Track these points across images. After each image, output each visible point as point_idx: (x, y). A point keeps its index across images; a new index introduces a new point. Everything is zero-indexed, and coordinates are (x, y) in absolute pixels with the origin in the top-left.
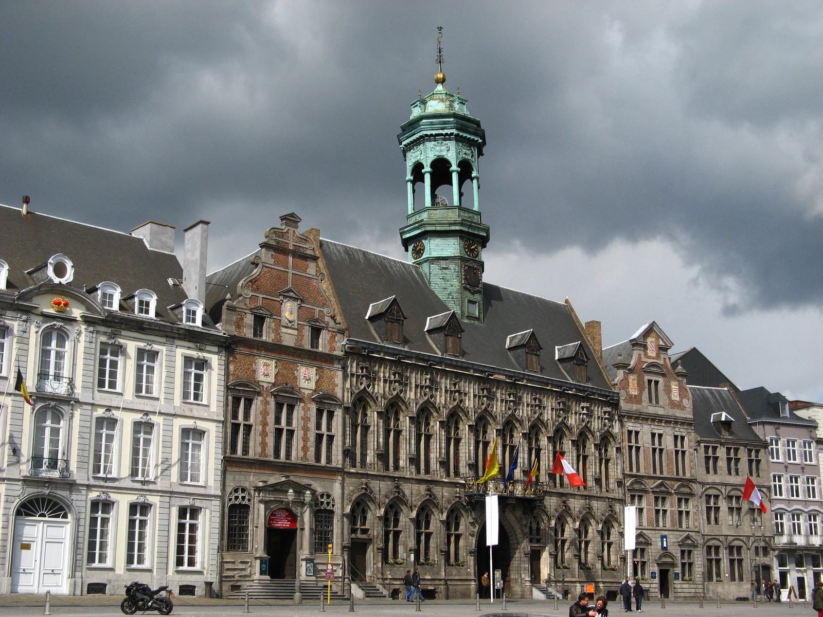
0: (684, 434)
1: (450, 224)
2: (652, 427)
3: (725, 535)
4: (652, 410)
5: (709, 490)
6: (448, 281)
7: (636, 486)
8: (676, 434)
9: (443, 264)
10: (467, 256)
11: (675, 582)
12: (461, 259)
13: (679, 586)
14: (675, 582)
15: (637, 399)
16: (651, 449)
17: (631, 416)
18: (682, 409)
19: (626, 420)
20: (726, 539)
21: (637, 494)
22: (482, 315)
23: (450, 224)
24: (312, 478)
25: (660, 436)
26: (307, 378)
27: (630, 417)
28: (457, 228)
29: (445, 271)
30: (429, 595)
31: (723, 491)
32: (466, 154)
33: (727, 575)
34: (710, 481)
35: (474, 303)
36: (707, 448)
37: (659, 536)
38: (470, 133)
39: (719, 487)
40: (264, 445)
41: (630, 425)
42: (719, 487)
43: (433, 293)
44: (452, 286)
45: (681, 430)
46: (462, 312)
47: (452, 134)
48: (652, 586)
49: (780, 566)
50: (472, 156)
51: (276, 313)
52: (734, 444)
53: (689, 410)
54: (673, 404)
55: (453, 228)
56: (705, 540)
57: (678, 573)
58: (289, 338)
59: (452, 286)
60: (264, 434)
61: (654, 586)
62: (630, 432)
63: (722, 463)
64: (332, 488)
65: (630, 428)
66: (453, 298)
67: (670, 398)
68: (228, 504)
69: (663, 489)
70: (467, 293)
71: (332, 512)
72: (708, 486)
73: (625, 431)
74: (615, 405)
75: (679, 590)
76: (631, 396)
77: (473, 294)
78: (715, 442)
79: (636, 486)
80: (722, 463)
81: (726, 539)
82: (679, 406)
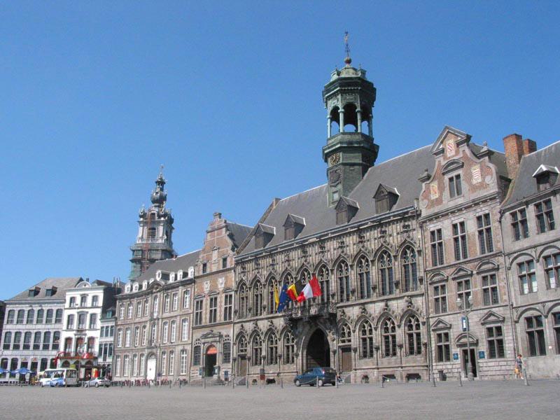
0: (487, 212)
2: (453, 219)
3: (541, 303)
4: (452, 204)
5: (520, 258)
7: (436, 279)
8: (477, 215)
11: (479, 361)
13: (485, 365)
14: (479, 361)
15: (439, 201)
16: (452, 240)
17: (431, 219)
18: (484, 188)
19: (428, 223)
20: (544, 307)
21: (439, 285)
24: (221, 329)
25: (462, 224)
26: (221, 282)
27: (431, 219)
30: (271, 381)
31: (533, 254)
33: (550, 347)
34: (517, 248)
35: (336, 192)
36: (514, 215)
37: (460, 318)
39: (528, 252)
40: (206, 318)
41: (432, 227)
42: (528, 252)
45: (484, 209)
48: (454, 366)
49: (542, 330)
51: (209, 259)
52: (541, 198)
53: (493, 185)
54: (474, 188)
56: (519, 313)
57: (483, 352)
58: (214, 269)
60: (206, 313)
61: (458, 366)
62: (433, 233)
63: (532, 223)
64: (230, 331)
65: (432, 230)
67: (471, 184)
68: (194, 346)
69: (462, 273)
70: (333, 188)
71: (229, 343)
72: (515, 255)
73: (428, 234)
74: (417, 215)
75: (485, 369)
76: (433, 201)
77: (335, 186)
78: (521, 204)
79: (436, 279)
80: (532, 223)
81: (544, 307)
82: (482, 185)
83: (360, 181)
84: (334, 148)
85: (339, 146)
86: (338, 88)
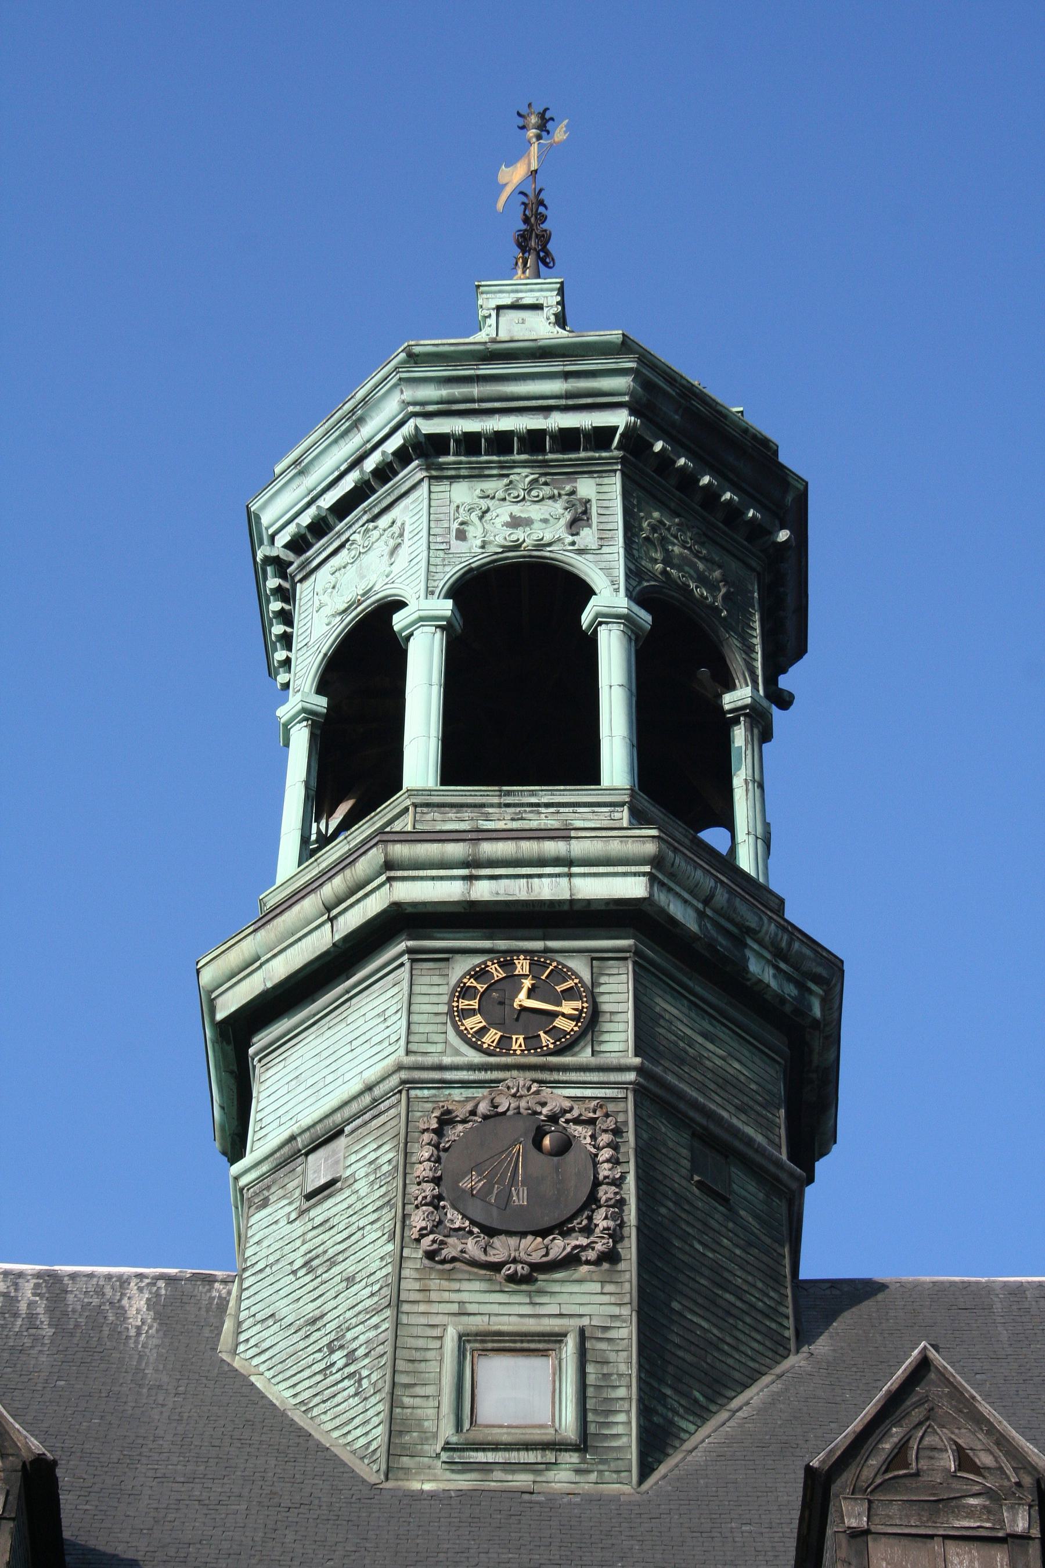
1: (330, 911)
6: (332, 1262)
9: (317, 1169)
10: (475, 1057)
12: (411, 1078)
22: (624, 1428)
23: (330, 911)
28: (372, 906)
29: (319, 1214)
32: (516, 522)
35: (536, 1344)
38: (547, 410)
43: (241, 1383)
44: (350, 1281)
46: (396, 1427)
47: (403, 456)
50: (579, 520)
55: (352, 919)
59: (350, 1281)
66: (351, 1358)
77: (528, 1278)
83: (780, 1350)
84: (548, 888)
85: (632, 887)
86: (620, 419)
